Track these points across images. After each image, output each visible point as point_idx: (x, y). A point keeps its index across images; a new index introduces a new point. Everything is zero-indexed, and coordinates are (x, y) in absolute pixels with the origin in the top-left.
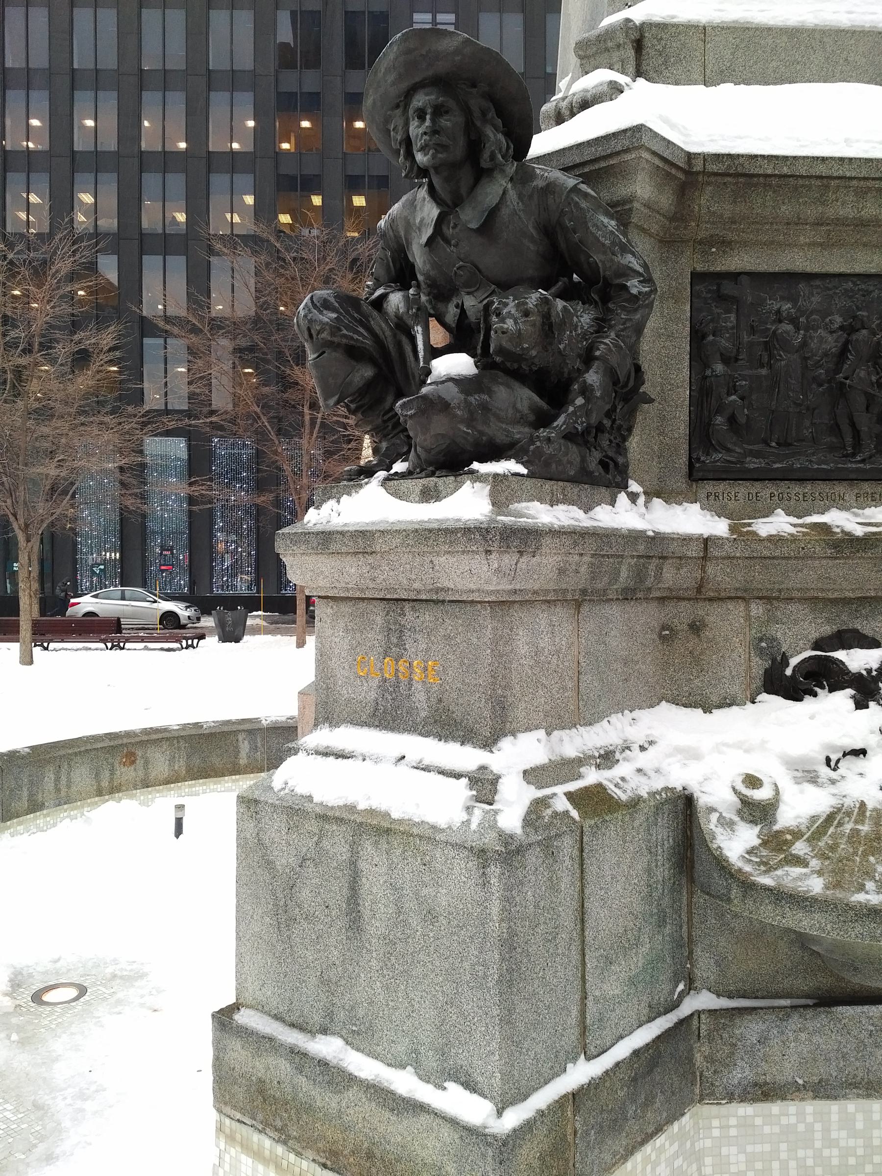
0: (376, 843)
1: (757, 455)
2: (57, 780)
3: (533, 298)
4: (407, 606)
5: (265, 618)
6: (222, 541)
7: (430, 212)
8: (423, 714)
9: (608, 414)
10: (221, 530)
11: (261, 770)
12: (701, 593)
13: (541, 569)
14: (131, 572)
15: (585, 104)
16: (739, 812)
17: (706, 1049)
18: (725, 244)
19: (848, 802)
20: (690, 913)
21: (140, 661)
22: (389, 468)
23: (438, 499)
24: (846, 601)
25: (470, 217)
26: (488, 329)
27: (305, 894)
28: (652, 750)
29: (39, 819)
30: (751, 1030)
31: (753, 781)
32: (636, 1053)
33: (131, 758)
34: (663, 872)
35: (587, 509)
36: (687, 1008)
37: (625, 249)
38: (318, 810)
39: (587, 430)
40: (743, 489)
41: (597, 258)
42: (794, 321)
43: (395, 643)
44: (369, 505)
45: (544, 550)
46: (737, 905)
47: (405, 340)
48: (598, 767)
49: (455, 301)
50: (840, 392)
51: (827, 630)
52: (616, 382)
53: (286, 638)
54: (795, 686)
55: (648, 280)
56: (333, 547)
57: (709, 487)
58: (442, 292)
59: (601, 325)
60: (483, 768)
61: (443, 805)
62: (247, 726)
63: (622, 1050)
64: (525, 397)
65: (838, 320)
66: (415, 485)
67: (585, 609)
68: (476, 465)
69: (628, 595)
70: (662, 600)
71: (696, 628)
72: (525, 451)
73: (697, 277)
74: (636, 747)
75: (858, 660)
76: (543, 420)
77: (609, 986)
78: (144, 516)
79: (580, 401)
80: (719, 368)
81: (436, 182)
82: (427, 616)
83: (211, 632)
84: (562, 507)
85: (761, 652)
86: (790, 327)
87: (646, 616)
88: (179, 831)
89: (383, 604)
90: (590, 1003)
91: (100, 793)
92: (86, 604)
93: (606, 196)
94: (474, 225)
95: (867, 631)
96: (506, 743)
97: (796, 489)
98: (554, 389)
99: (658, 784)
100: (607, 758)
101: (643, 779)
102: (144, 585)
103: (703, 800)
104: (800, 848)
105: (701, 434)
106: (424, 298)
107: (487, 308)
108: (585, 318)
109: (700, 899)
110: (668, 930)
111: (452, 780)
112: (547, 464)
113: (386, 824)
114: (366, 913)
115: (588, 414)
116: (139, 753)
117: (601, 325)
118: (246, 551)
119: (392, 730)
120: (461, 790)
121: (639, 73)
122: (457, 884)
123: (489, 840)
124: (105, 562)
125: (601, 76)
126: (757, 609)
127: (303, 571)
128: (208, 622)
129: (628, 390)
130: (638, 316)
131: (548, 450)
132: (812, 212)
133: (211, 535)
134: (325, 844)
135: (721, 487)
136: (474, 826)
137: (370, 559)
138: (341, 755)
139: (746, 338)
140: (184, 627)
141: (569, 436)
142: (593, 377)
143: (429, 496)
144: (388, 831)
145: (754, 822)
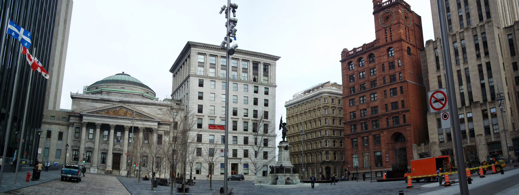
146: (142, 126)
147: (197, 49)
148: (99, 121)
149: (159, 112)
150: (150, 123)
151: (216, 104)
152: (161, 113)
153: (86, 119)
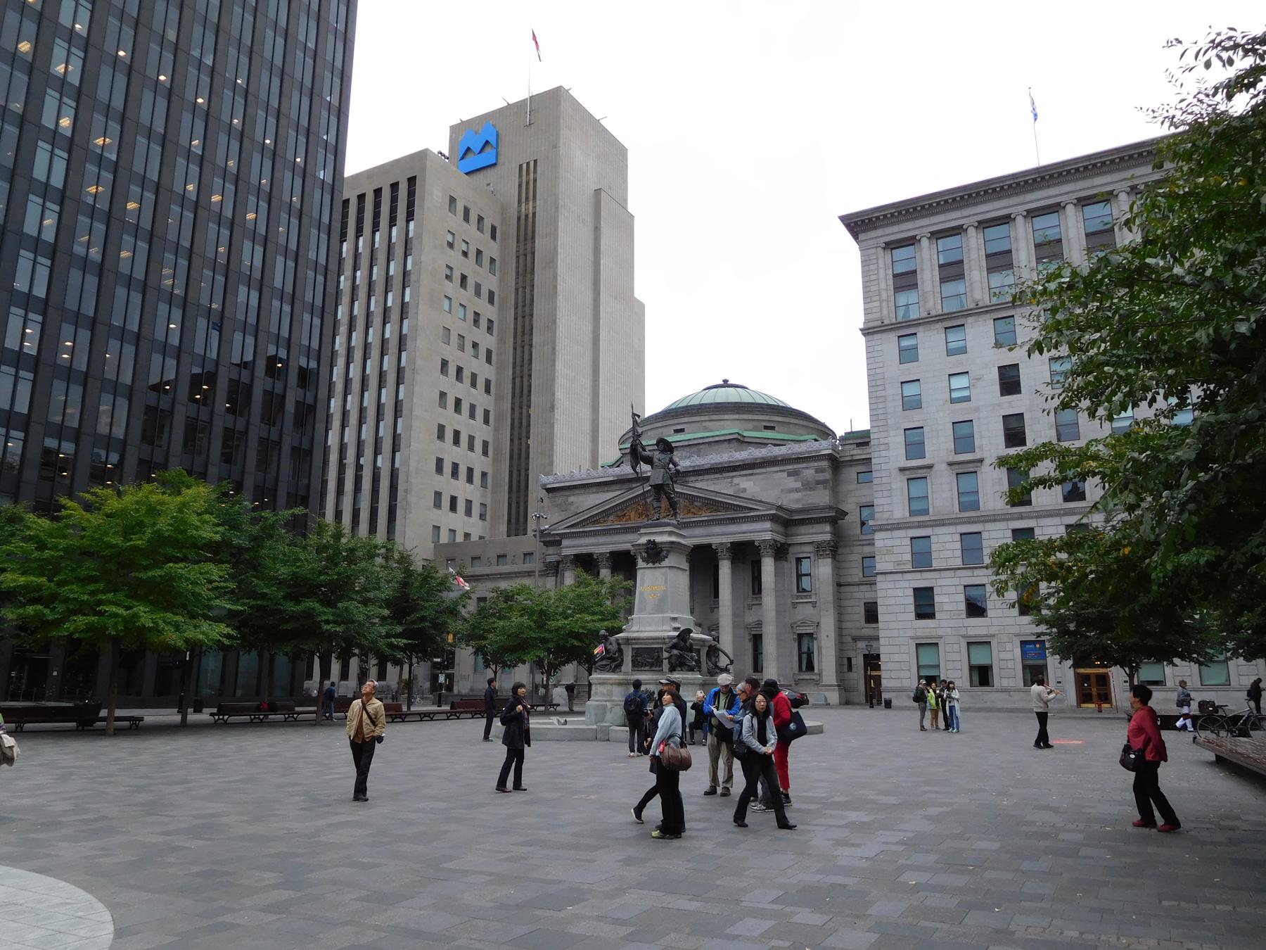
146: (724, 540)
147: (879, 232)
148: (602, 546)
149: (792, 483)
150: (745, 527)
151: (977, 409)
152: (799, 485)
153: (570, 548)
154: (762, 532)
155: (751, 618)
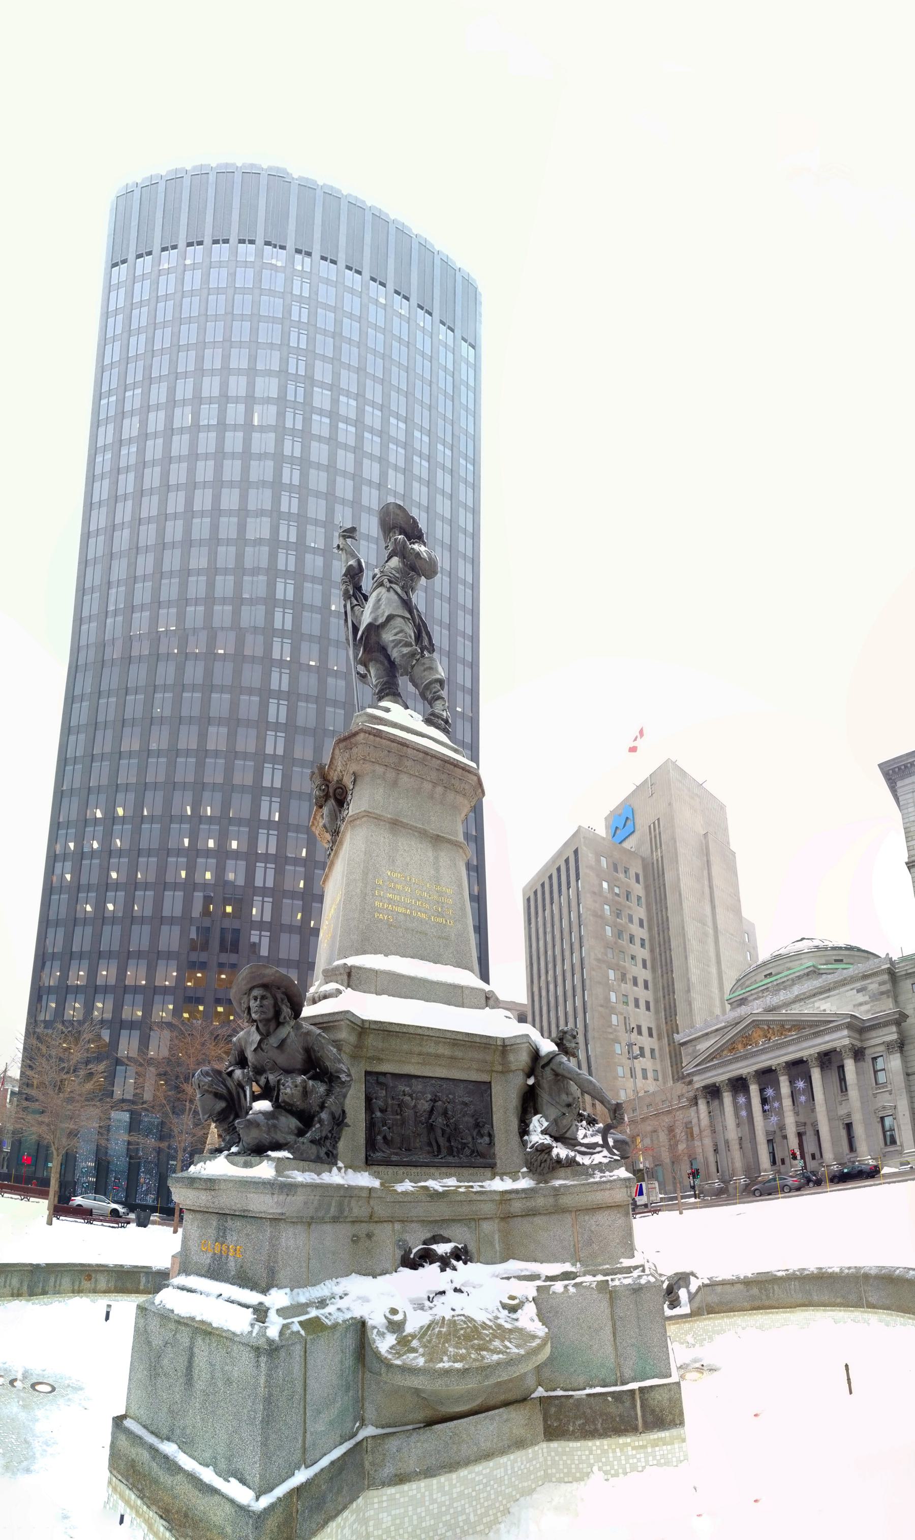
0: (204, 1339)
1: (396, 1154)
2: (55, 1281)
3: (300, 1079)
4: (229, 1217)
5: (159, 1217)
6: (143, 1178)
7: (257, 1037)
8: (233, 1273)
9: (330, 1131)
10: (143, 1172)
11: (150, 1293)
12: (371, 1219)
13: (295, 1204)
14: (100, 1189)
15: (325, 997)
16: (387, 1328)
17: (370, 1458)
18: (380, 1060)
19: (437, 1317)
20: (363, 1383)
21: (99, 1231)
22: (229, 1150)
23: (251, 1167)
24: (436, 1222)
25: (273, 1041)
26: (279, 1090)
27: (165, 1362)
28: (345, 1298)
29: (45, 1299)
30: (393, 1444)
31: (394, 1311)
32: (333, 1463)
33: (89, 1278)
34: (349, 1362)
35: (319, 1174)
36: (359, 1437)
37: (340, 1061)
38: (176, 1318)
39: (321, 1139)
40: (391, 1170)
41: (328, 1064)
42: (411, 1096)
43: (222, 1235)
44: (218, 1167)
45: (299, 1193)
46: (384, 1377)
47: (241, 1091)
48: (317, 1308)
49: (264, 1075)
50: (431, 1128)
51: (429, 1235)
52: (334, 1118)
53: (168, 1228)
54: (413, 1263)
55: (349, 1075)
56: (196, 1185)
57: (375, 1168)
58: (259, 1071)
59: (329, 1092)
60: (261, 1304)
61: (239, 1322)
62: (145, 1270)
63: (325, 1462)
64: (294, 1123)
65: (429, 1097)
66: (241, 1159)
67: (313, 1226)
68: (269, 1153)
69: (335, 1220)
70: (353, 1222)
71: (369, 1236)
72: (293, 1148)
73: (367, 1073)
74: (337, 1297)
75: (442, 1249)
76: (301, 1133)
77: (318, 1426)
78: (109, 1162)
79: (318, 1126)
80: (379, 1114)
81: (260, 1025)
82: (238, 1224)
83: (133, 1221)
84: (307, 1173)
85: (400, 1247)
86: (409, 1098)
87: (345, 1231)
88: (107, 1318)
89: (217, 1216)
90: (308, 1435)
91: (73, 1292)
92: (78, 1200)
93: (332, 1037)
94: (275, 1045)
95: (446, 1235)
96: (274, 1291)
97: (414, 1170)
98: (306, 1119)
99: (348, 1316)
100: (322, 1303)
101: (340, 1314)
102: (105, 1195)
103: (370, 1323)
104: (415, 1343)
105: (371, 1144)
106: (251, 1073)
107: (279, 1081)
108: (321, 1088)
109: (368, 1375)
110: (351, 1394)
111: (245, 1309)
112: (302, 1154)
113: (209, 1330)
114: (196, 1377)
115: (321, 1131)
116: (93, 1276)
117: (329, 1092)
118: (153, 1183)
119: (217, 1280)
120: (249, 1314)
121: (349, 986)
122: (243, 1365)
123: (262, 1342)
124: (89, 1182)
125: (332, 986)
126: (397, 1226)
127: (180, 1195)
128: (132, 1216)
129: (339, 1121)
130: (344, 1090)
131: (303, 1148)
132: (417, 1049)
133: (138, 1174)
134: (178, 1336)
135: (381, 1168)
136: (254, 1334)
137: (213, 1193)
138: (190, 1290)
139: (390, 1102)
140: (121, 1217)
141: (312, 1142)
142: (324, 1115)
143: (247, 1165)
144: (210, 1333)
145: (394, 1332)
150: (827, 1038)
154: (841, 1039)
155: (842, 1111)
